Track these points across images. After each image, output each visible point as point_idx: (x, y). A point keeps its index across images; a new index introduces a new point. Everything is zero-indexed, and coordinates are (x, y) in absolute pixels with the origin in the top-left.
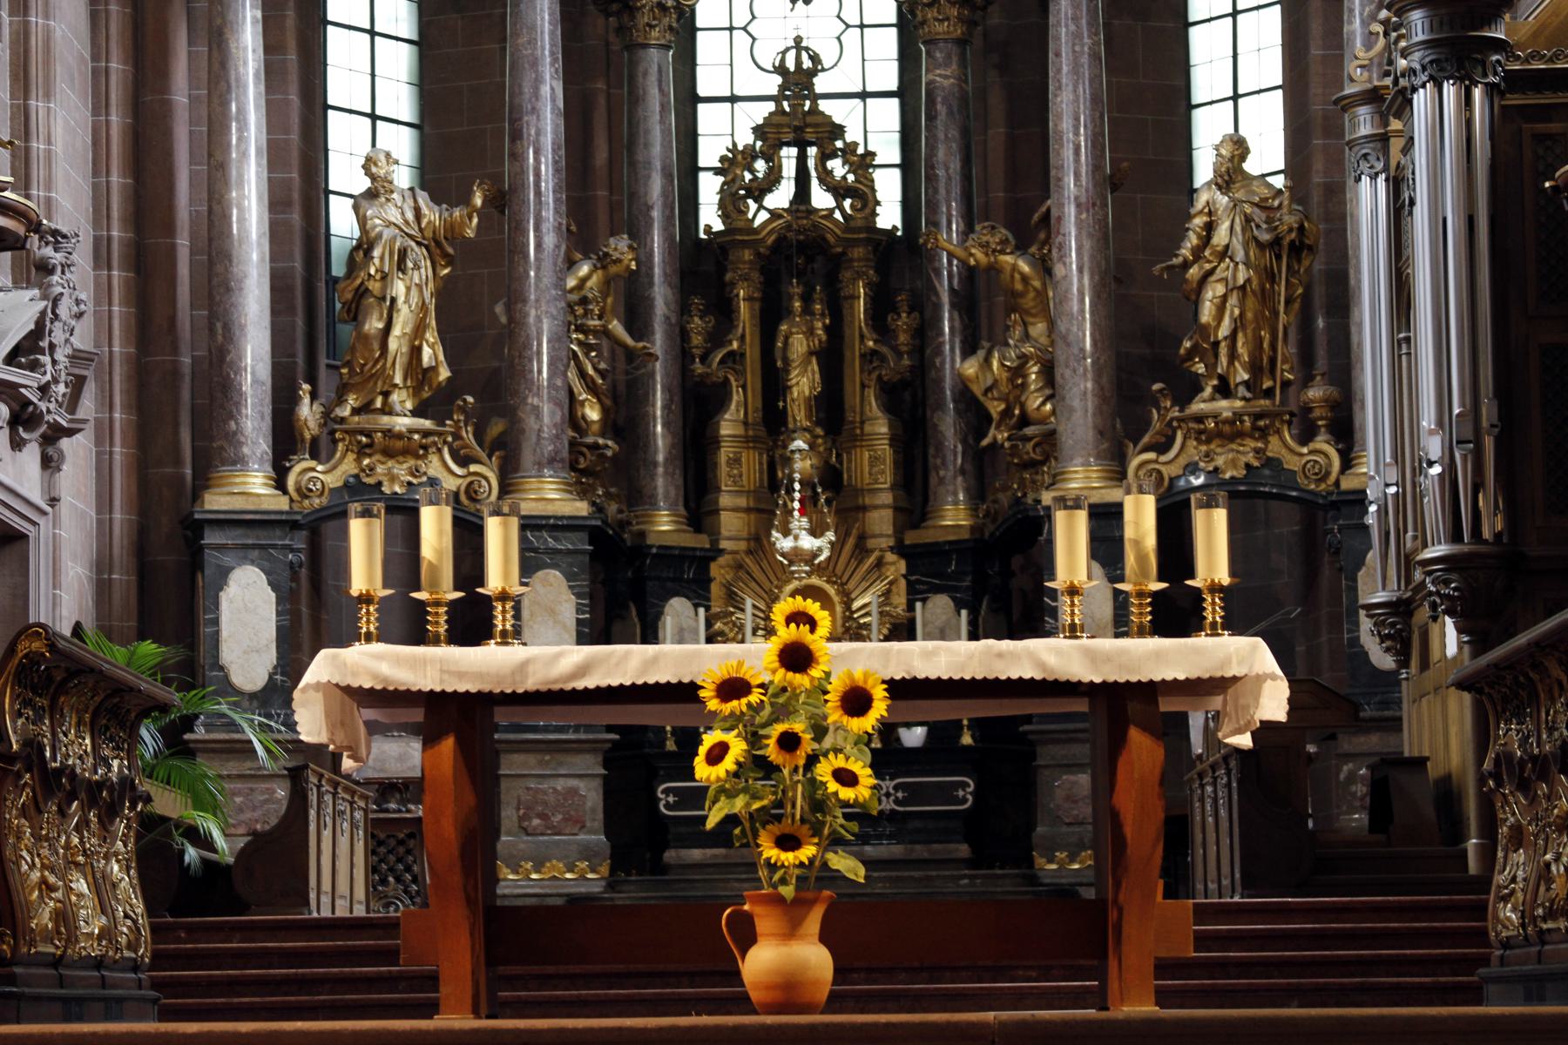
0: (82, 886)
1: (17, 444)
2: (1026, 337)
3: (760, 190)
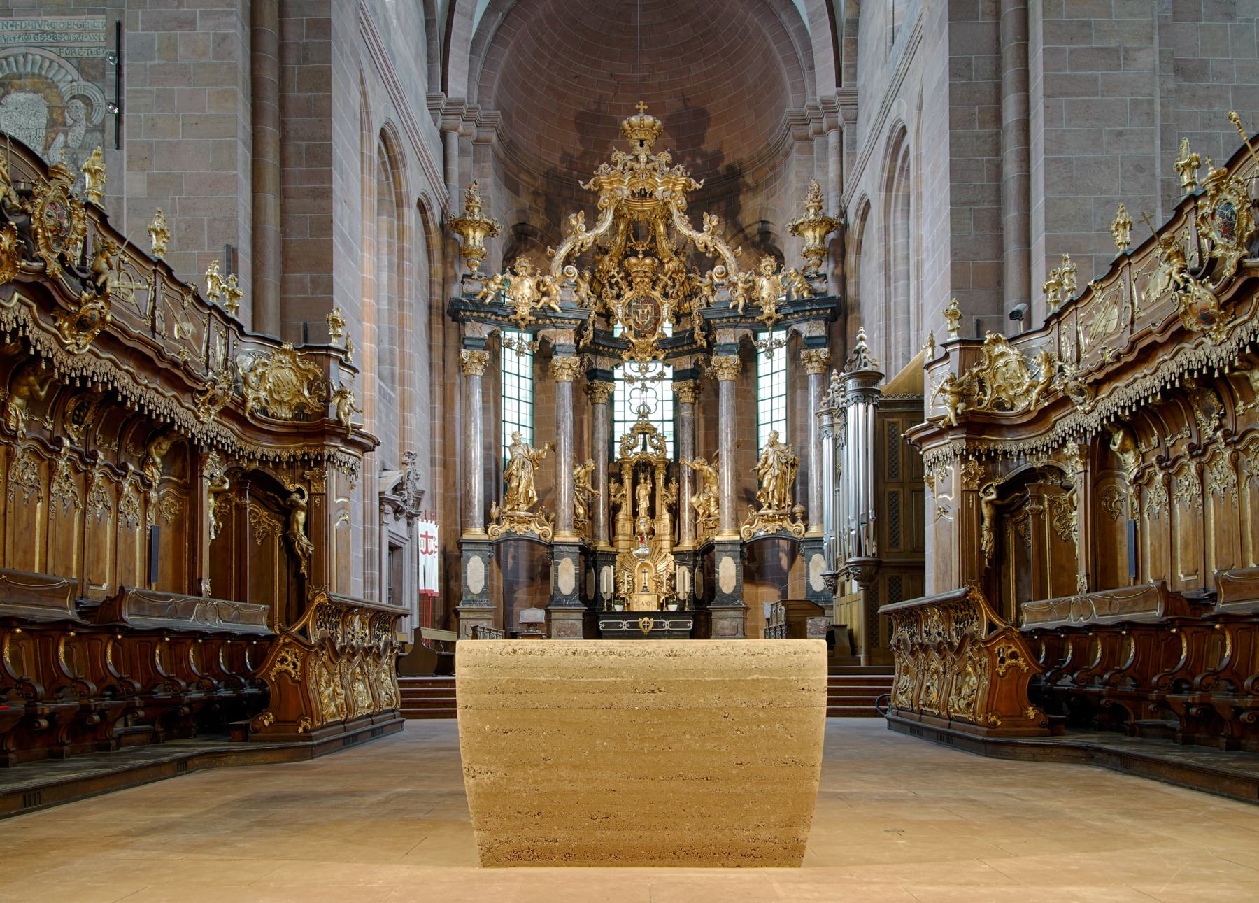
0: (360, 687)
1: (397, 519)
2: (710, 491)
3: (631, 448)
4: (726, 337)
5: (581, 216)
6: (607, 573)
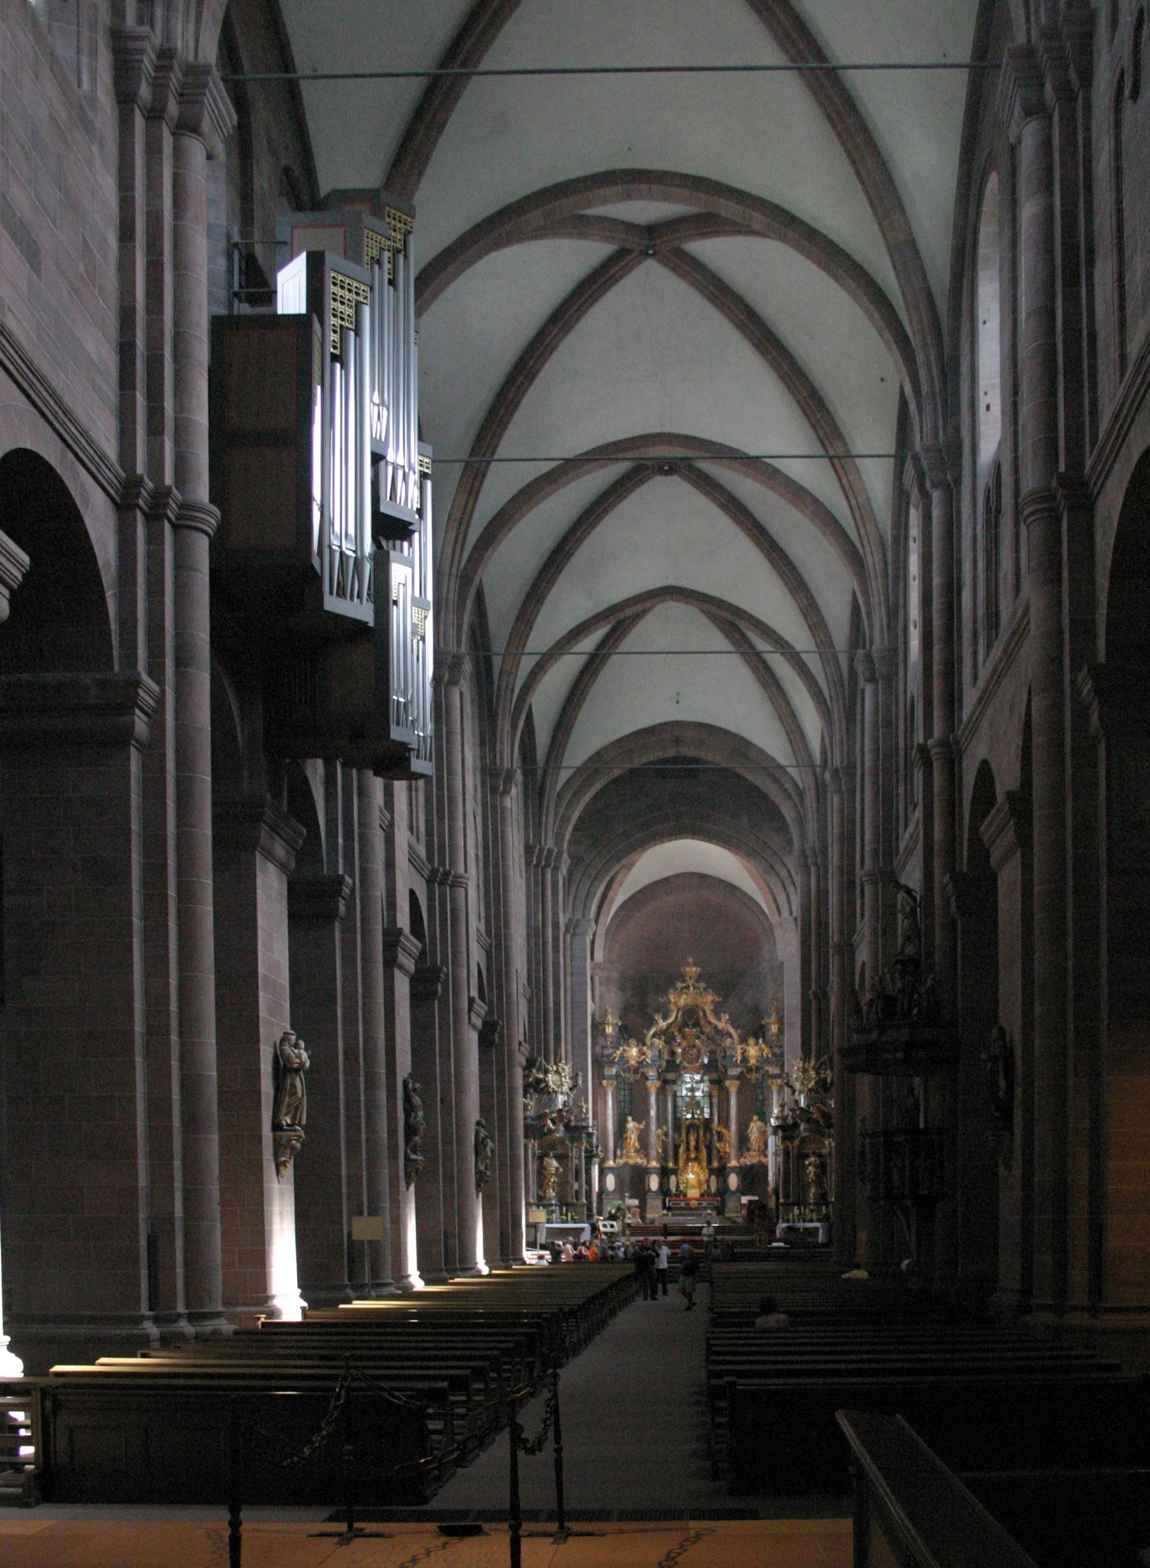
5: (660, 1015)
6: (673, 1179)
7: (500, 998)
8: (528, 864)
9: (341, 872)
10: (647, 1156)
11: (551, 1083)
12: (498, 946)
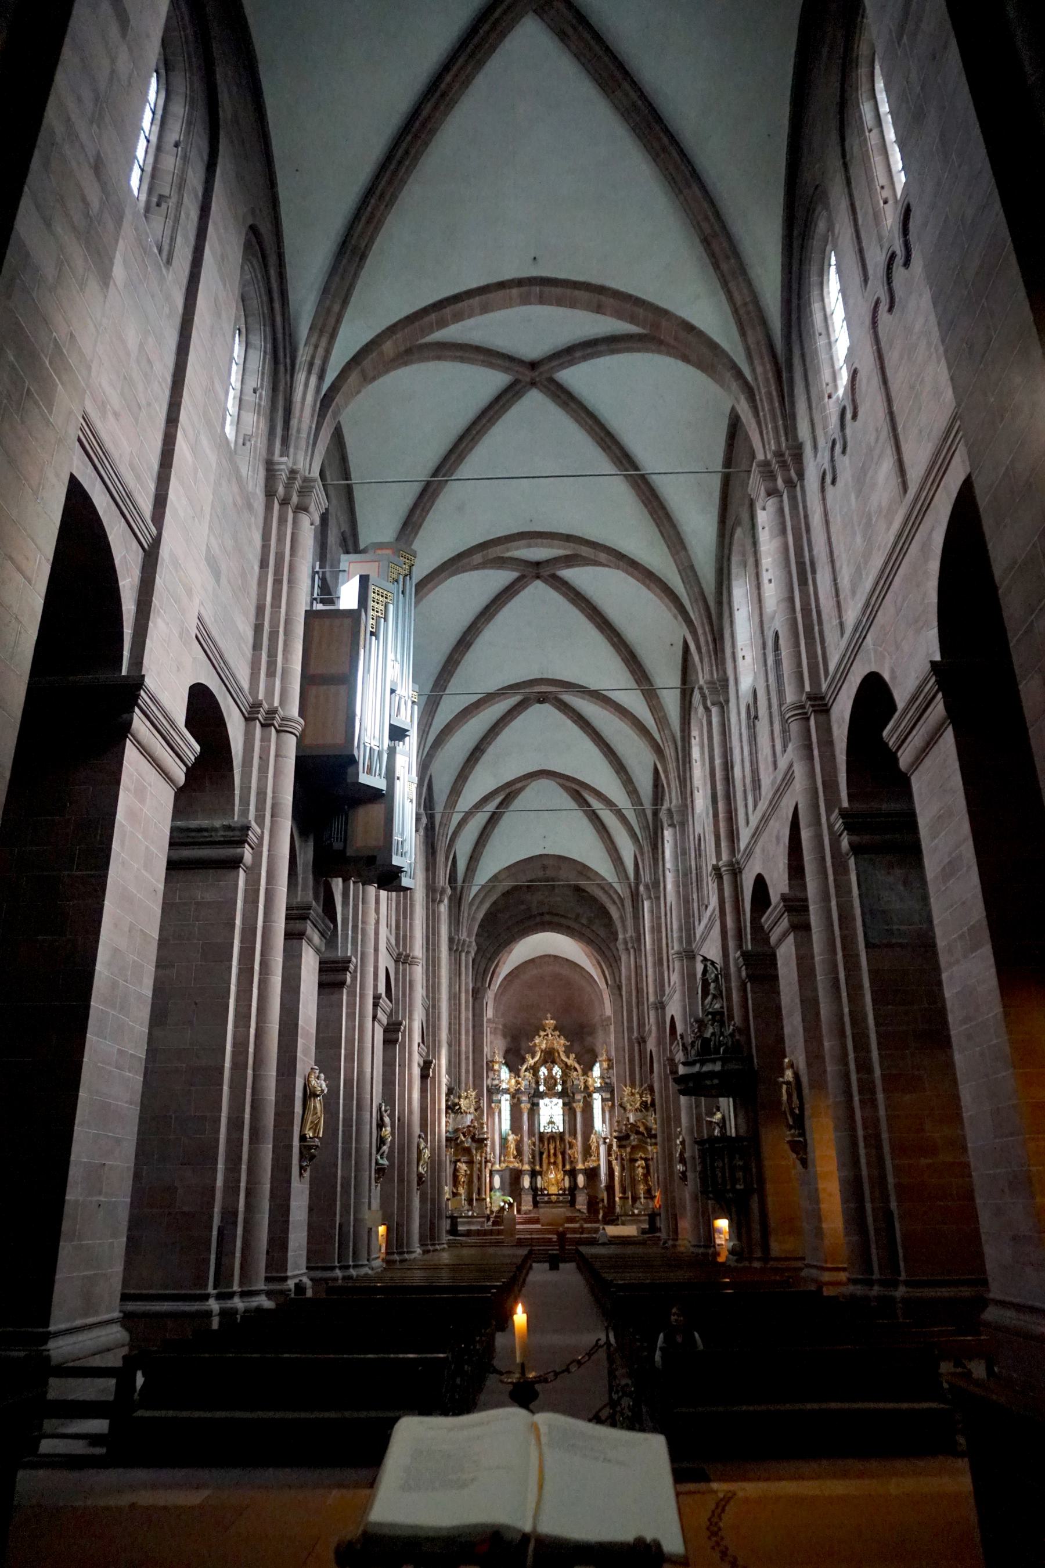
4: (578, 1097)
6: (539, 1178)
7: (434, 1041)
8: (450, 949)
9: (349, 954)
10: (521, 1161)
11: (462, 1106)
12: (434, 1007)
